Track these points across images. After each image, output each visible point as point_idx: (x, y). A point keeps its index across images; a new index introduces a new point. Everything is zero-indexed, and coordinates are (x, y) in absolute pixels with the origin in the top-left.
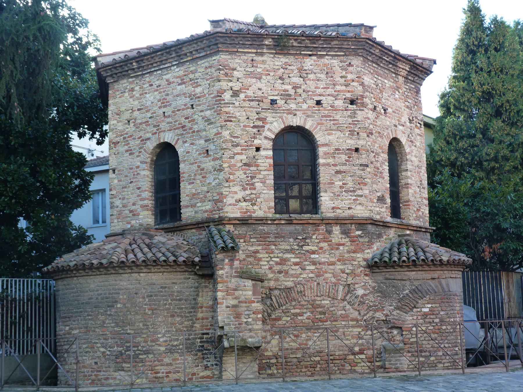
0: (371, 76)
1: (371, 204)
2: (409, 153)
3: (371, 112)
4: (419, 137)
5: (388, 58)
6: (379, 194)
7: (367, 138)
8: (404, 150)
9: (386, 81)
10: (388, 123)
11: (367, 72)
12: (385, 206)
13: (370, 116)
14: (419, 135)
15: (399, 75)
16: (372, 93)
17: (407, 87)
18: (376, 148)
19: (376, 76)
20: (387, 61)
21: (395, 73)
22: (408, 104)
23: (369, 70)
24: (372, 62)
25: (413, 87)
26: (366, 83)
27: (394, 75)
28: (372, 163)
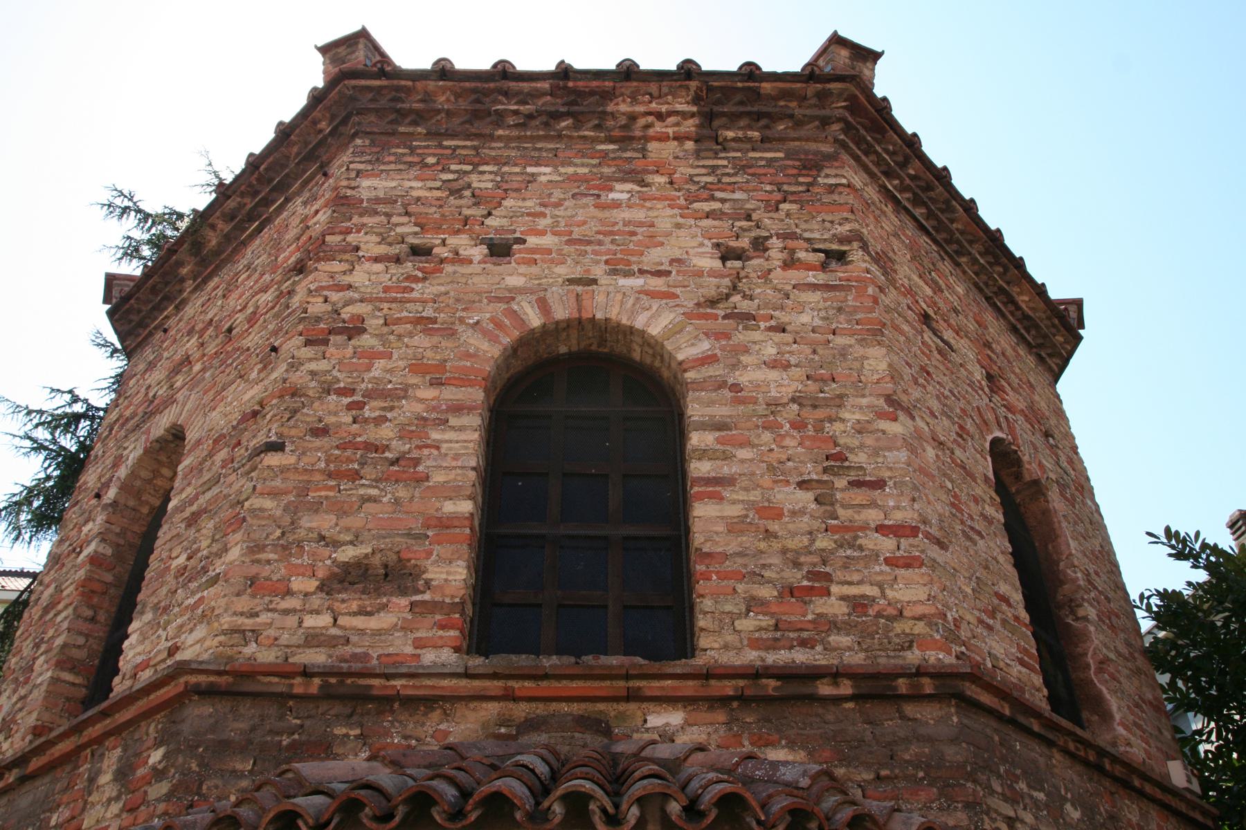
0: (414, 172)
1: (244, 603)
2: (707, 360)
3: (379, 267)
4: (814, 297)
5: (524, 103)
6: (347, 554)
7: (307, 352)
8: (671, 356)
9: (529, 170)
10: (515, 281)
11: (393, 166)
12: (404, 602)
13: (359, 277)
14: (814, 287)
15: (647, 139)
16: (407, 214)
17: (725, 163)
18: (376, 372)
19: (453, 167)
20: (530, 117)
21: (610, 140)
22: (716, 205)
23: (410, 159)
24: (430, 135)
25: (781, 155)
26: (365, 195)
27: (612, 147)
28: (321, 431)
